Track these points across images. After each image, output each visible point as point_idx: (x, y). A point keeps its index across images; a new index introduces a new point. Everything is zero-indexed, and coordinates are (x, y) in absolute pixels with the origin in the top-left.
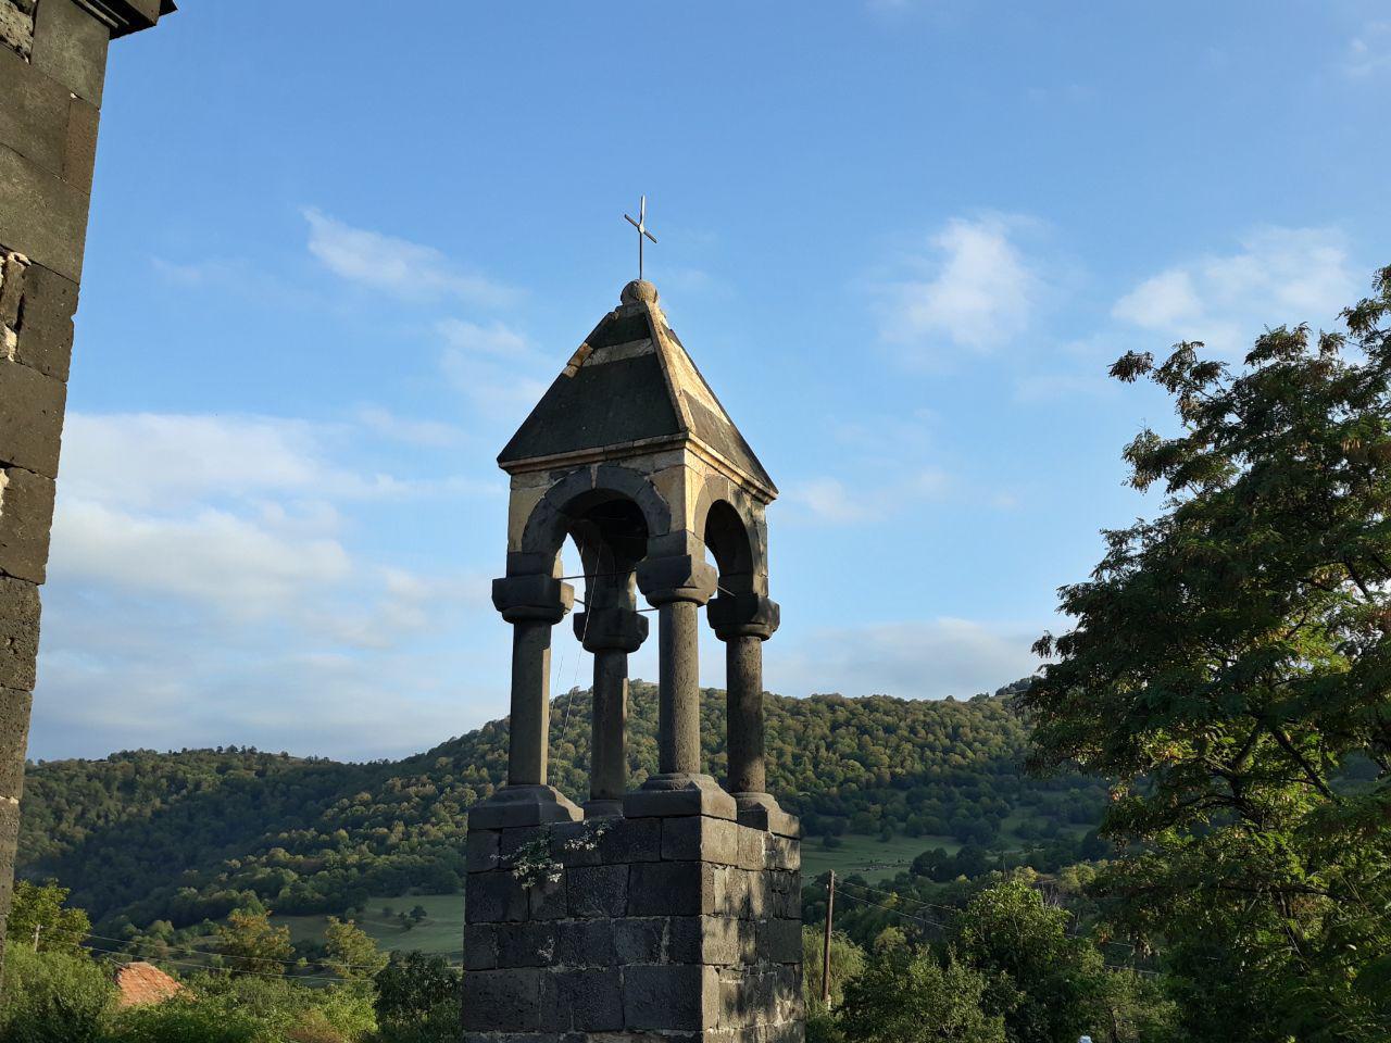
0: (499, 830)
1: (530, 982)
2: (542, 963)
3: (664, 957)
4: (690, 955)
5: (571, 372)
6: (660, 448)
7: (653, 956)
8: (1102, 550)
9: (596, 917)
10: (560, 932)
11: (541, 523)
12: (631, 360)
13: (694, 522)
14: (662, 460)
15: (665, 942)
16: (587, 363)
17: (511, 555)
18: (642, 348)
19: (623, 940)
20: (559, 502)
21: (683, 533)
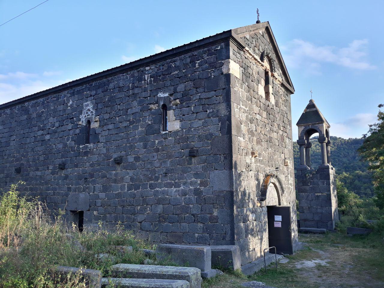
0: (301, 170)
1: (307, 188)
2: (309, 185)
3: (325, 185)
4: (329, 184)
5: (304, 112)
6: (320, 123)
7: (324, 184)
8: (368, 128)
9: (315, 180)
10: (311, 182)
11: (303, 133)
12: (313, 111)
13: (325, 133)
14: (320, 125)
15: (325, 183)
16: (306, 111)
17: (299, 137)
18: (314, 109)
19: (320, 183)
20: (306, 130)
21: (324, 134)
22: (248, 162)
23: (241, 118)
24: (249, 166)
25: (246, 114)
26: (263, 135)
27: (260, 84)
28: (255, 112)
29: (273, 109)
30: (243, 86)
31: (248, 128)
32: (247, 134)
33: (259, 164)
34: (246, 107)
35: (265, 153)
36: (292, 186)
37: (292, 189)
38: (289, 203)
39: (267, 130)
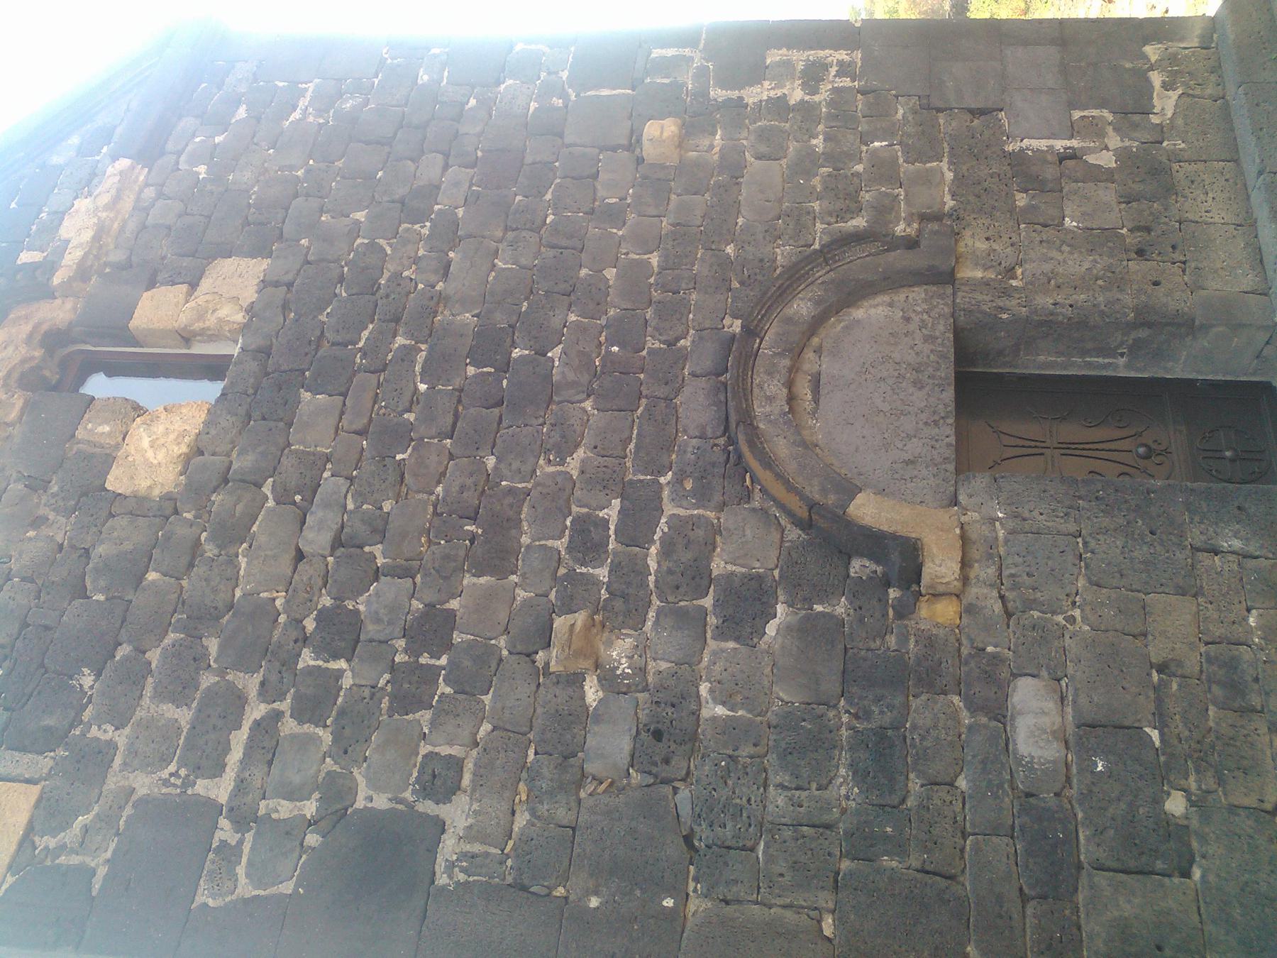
22: (626, 744)
23: (310, 808)
24: (658, 735)
25: (289, 726)
26: (452, 457)
27: (108, 460)
28: (284, 564)
29: (290, 285)
30: (94, 732)
31: (385, 704)
32: (425, 716)
33: (653, 565)
34: (239, 701)
35: (580, 453)
36: (825, 67)
37: (844, 69)
38: (939, 110)
39: (423, 387)
